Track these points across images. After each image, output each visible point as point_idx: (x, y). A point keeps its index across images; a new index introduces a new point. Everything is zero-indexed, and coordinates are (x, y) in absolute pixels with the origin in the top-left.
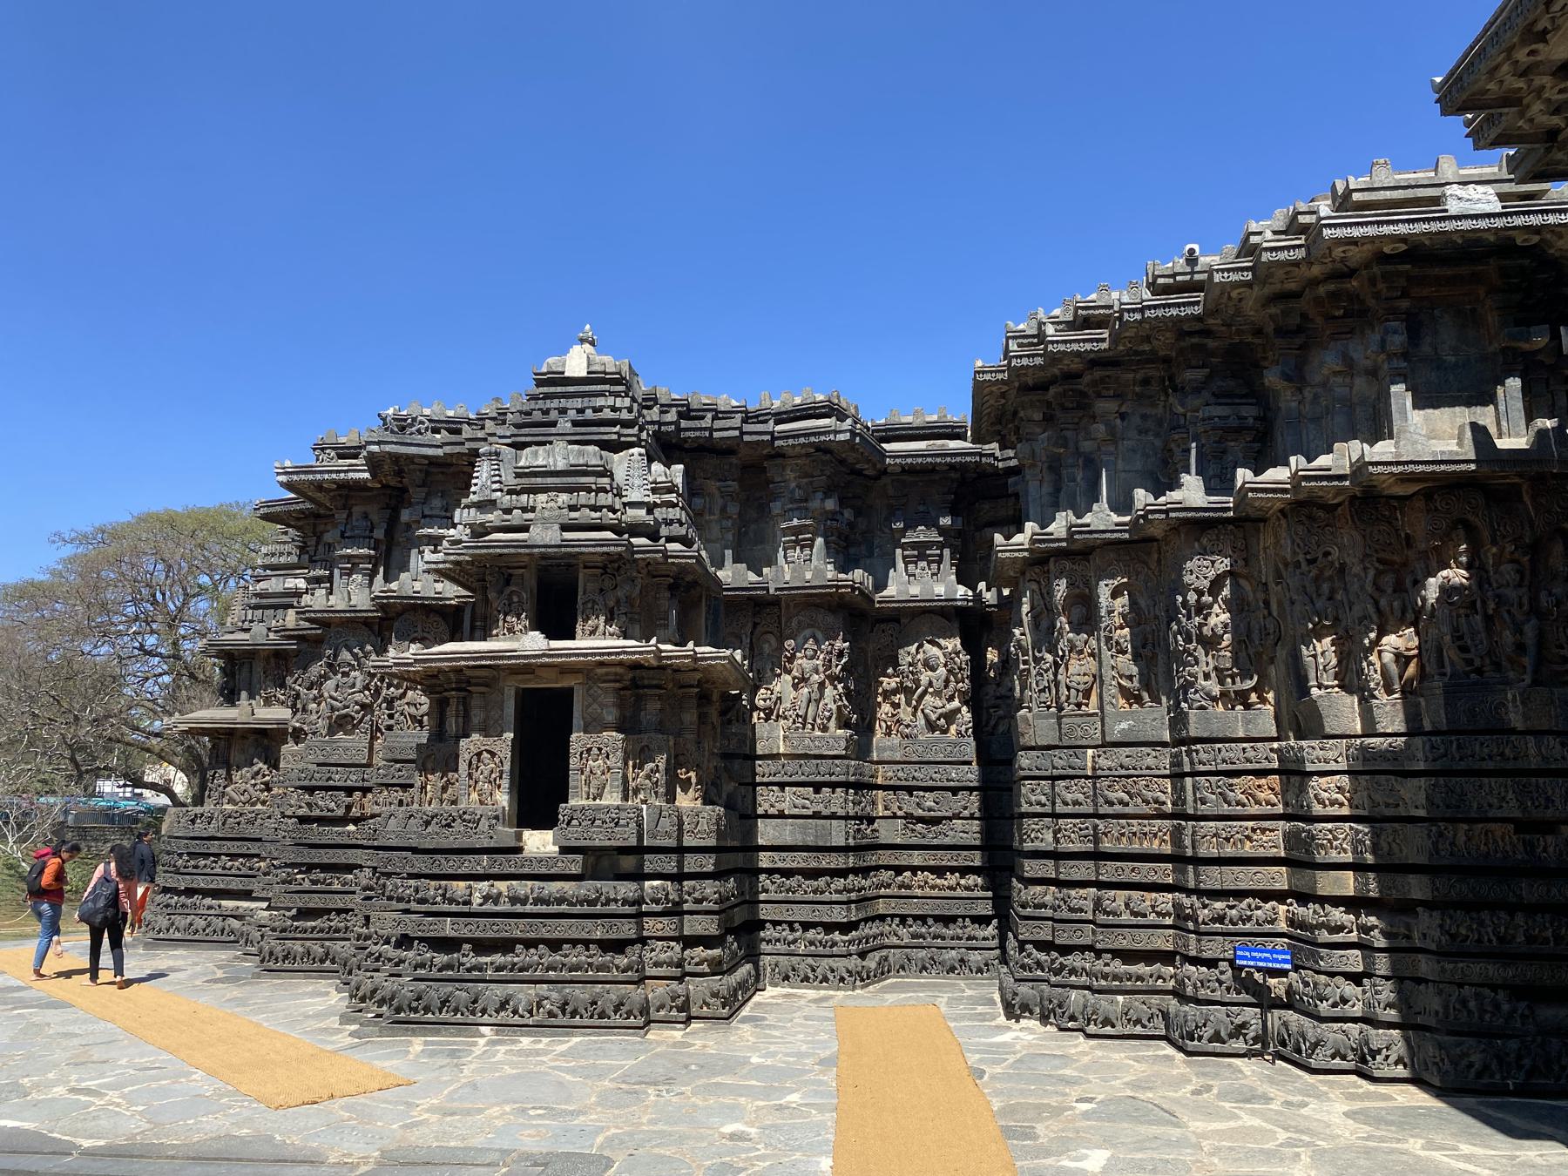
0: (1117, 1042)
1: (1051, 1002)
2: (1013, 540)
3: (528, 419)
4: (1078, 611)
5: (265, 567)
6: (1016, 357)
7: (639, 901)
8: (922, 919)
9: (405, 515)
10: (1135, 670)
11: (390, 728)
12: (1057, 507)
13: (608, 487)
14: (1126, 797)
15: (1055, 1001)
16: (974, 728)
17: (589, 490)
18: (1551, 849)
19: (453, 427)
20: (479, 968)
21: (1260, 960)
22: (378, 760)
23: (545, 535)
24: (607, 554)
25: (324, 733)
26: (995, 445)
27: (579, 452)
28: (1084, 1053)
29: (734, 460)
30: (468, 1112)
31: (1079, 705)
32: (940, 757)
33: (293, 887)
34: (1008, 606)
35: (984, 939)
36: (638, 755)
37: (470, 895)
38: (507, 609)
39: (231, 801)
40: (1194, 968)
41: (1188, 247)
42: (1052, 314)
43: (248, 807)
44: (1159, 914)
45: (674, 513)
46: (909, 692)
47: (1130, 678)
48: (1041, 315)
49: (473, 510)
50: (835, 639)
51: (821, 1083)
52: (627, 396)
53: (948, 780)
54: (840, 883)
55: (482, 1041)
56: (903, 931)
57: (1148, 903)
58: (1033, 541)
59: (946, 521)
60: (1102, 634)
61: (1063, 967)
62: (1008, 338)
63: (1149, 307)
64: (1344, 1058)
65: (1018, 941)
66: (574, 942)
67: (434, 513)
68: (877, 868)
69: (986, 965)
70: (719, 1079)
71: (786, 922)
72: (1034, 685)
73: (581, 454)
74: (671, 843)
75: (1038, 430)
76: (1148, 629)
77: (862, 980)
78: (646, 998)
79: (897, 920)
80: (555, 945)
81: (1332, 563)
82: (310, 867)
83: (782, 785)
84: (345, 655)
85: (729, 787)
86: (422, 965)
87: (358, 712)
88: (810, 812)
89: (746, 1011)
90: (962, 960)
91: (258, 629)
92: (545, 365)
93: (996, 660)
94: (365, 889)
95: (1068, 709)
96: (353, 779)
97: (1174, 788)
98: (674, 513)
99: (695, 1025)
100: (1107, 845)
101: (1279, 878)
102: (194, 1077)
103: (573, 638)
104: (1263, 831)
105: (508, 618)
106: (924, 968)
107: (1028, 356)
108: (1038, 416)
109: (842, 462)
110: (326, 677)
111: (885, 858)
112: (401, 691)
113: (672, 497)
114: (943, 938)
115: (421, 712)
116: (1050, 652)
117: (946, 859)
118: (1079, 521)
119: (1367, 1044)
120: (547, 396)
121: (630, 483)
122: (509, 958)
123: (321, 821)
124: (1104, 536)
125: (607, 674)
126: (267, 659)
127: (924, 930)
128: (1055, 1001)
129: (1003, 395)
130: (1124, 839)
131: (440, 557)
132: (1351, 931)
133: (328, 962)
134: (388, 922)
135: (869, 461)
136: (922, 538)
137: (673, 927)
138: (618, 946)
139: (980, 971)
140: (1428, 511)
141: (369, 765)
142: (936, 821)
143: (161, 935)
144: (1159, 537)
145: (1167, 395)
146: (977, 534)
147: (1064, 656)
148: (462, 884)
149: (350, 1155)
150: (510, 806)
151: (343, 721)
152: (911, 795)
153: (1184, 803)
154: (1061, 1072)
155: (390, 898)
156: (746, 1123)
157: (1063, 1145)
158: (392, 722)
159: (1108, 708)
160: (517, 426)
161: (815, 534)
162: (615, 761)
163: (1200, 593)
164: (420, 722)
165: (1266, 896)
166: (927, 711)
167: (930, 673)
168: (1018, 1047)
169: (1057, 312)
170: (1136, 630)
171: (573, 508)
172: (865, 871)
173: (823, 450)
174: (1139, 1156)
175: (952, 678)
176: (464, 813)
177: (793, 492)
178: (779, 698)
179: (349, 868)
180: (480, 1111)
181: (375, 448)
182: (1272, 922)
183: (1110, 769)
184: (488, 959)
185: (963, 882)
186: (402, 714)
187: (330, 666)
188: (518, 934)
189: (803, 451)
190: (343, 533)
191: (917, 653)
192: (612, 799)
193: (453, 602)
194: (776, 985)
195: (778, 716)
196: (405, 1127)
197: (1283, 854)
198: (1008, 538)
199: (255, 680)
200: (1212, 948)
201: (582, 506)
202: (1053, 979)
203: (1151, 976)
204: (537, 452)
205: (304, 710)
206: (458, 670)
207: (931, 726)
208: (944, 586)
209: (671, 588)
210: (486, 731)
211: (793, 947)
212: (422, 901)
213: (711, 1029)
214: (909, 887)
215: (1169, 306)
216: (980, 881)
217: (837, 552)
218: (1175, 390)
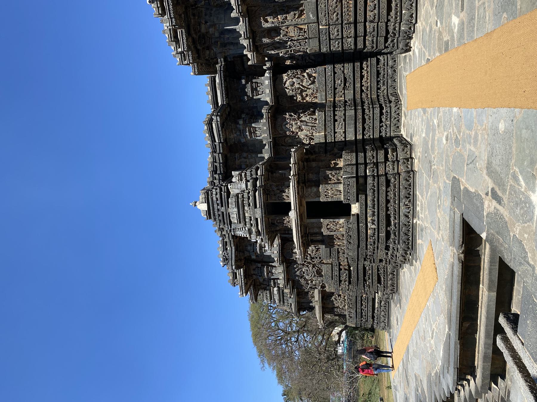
0: (418, 12)
1: (405, 36)
2: (250, 58)
4: (273, 34)
5: (271, 299)
6: (189, 61)
7: (374, 176)
8: (378, 82)
9: (254, 257)
10: (292, 13)
11: (320, 258)
12: (238, 43)
13: (242, 195)
14: (335, 14)
15: (405, 35)
16: (313, 68)
17: (243, 200)
19: (225, 244)
20: (395, 225)
22: (330, 261)
23: (259, 213)
24: (263, 193)
25: (322, 278)
26: (217, 66)
27: (231, 204)
28: (422, 24)
29: (229, 155)
30: (439, 223)
32: (324, 79)
33: (371, 285)
34: (271, 58)
35: (384, 60)
36: (326, 180)
37: (372, 228)
38: (282, 223)
39: (344, 306)
41: (148, 3)
42: (174, 49)
43: (346, 301)
45: (248, 173)
46: (302, 91)
47: (295, 14)
48: (174, 53)
49: (252, 236)
50: (285, 118)
51: (431, 113)
52: (212, 190)
53: (331, 76)
54: (367, 111)
55: (418, 222)
56: (382, 88)
57: (371, 4)
59: (243, 82)
60: (280, 25)
62: (183, 64)
63: (170, 16)
65: (384, 49)
67: (252, 248)
68: (361, 98)
69: (393, 59)
70: (430, 146)
71: (380, 129)
72: (299, 48)
73: (232, 204)
74: (355, 167)
75: (212, 52)
76: (278, 9)
77: (399, 101)
78: (404, 172)
79: (379, 91)
80: (388, 201)
82: (365, 280)
83: (335, 133)
84: (298, 273)
85: (336, 150)
86: (394, 242)
87: (315, 268)
88: (344, 123)
89: (409, 140)
90: (392, 68)
91: (290, 301)
92: (204, 216)
93: (290, 61)
94: (371, 263)
95: (306, 36)
96: (336, 268)
98: (248, 173)
99: (413, 156)
100: (352, 20)
102: (428, 305)
103: (290, 203)
105: (285, 223)
106: (394, 81)
107: (189, 57)
108: (208, 52)
109: (226, 119)
110: (305, 279)
111: (358, 96)
112: (308, 255)
113: (243, 174)
114: (384, 74)
115: (315, 249)
116: (287, 43)
117: (358, 75)
118: (243, 36)
121: (240, 188)
123: (350, 277)
124: (247, 27)
125: (301, 191)
126: (300, 298)
127: (382, 81)
128: (405, 35)
129: (201, 64)
131: (266, 245)
133: (394, 273)
134: (381, 254)
135: (225, 110)
136: (250, 90)
137: (382, 165)
138: (388, 182)
139: (395, 61)
141: (332, 264)
142: (345, 79)
144: (246, 7)
145: (198, 7)
146: (247, 70)
147: (288, 38)
148: (369, 231)
149: (451, 255)
150: (344, 219)
151: (319, 273)
152: (337, 88)
154: (428, 32)
155: (374, 253)
156: (443, 136)
157: (451, 31)
158: (318, 257)
159: (306, 22)
160: (224, 224)
161: (251, 127)
162: (329, 186)
166: (308, 84)
167: (295, 84)
168: (420, 47)
169: (173, 48)
170: (279, 13)
171: (249, 205)
172: (363, 103)
173: (223, 125)
174: (454, 5)
175: (297, 76)
176: (346, 232)
177: (237, 135)
178: (306, 135)
179: (364, 268)
180: (439, 219)
181: (234, 267)
183: (326, 20)
184: (392, 222)
185: (365, 69)
186: (316, 255)
187: (301, 278)
188: (384, 213)
189: (224, 132)
190: (260, 276)
191: (288, 89)
192: (341, 187)
193: (280, 241)
194: (400, 130)
195: (312, 136)
196: (443, 241)
198: (250, 60)
199: (307, 301)
201: (248, 202)
202: (397, 36)
204: (232, 217)
205: (315, 285)
207: (313, 82)
208: (266, 81)
209: (272, 173)
210: (321, 227)
211: (388, 126)
212: (374, 243)
213: (414, 150)
214: (368, 87)
215: (169, 9)
216: (365, 63)
217: (257, 119)
218: (196, 4)
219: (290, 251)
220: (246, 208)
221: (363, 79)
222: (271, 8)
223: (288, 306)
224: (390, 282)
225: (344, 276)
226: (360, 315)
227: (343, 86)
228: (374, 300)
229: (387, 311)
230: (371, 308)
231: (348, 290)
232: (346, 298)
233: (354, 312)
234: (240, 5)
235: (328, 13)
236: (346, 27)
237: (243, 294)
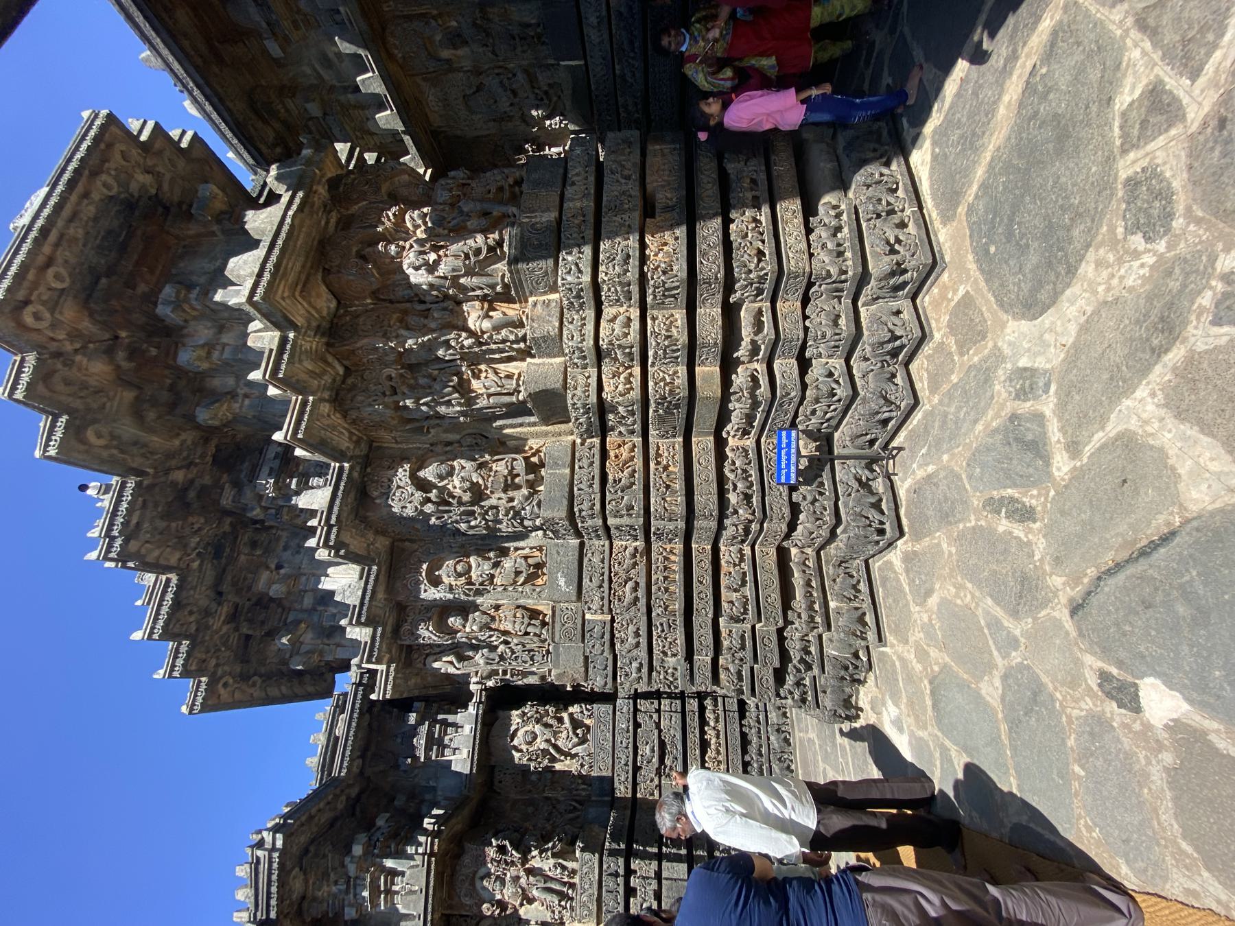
0: (883, 612)
14: (630, 584)
18: (669, 195)
21: (789, 460)
31: (544, 624)
32: (609, 736)
40: (800, 528)
44: (742, 560)
57: (731, 569)
58: (378, 662)
59: (412, 718)
61: (802, 661)
64: (894, 376)
81: (402, 376)
90: (778, 731)
97: (620, 538)
100: (678, 606)
101: (703, 444)
104: (658, 455)
114: (761, 746)
119: (882, 344)
127: (755, 765)
128: (843, 673)
130: (672, 588)
132: (756, 370)
136: (423, 742)
140: (339, 272)
142: (662, 744)
163: (428, 500)
165: (721, 457)
167: (538, 740)
182: (746, 451)
183: (602, 599)
185: (712, 724)
191: (521, 751)
197: (681, 439)
203: (804, 572)
207: (583, 741)
221: (707, 752)
222: (454, 550)
227: (657, 765)
234: (333, 526)
235: (611, 581)
236: (662, 624)
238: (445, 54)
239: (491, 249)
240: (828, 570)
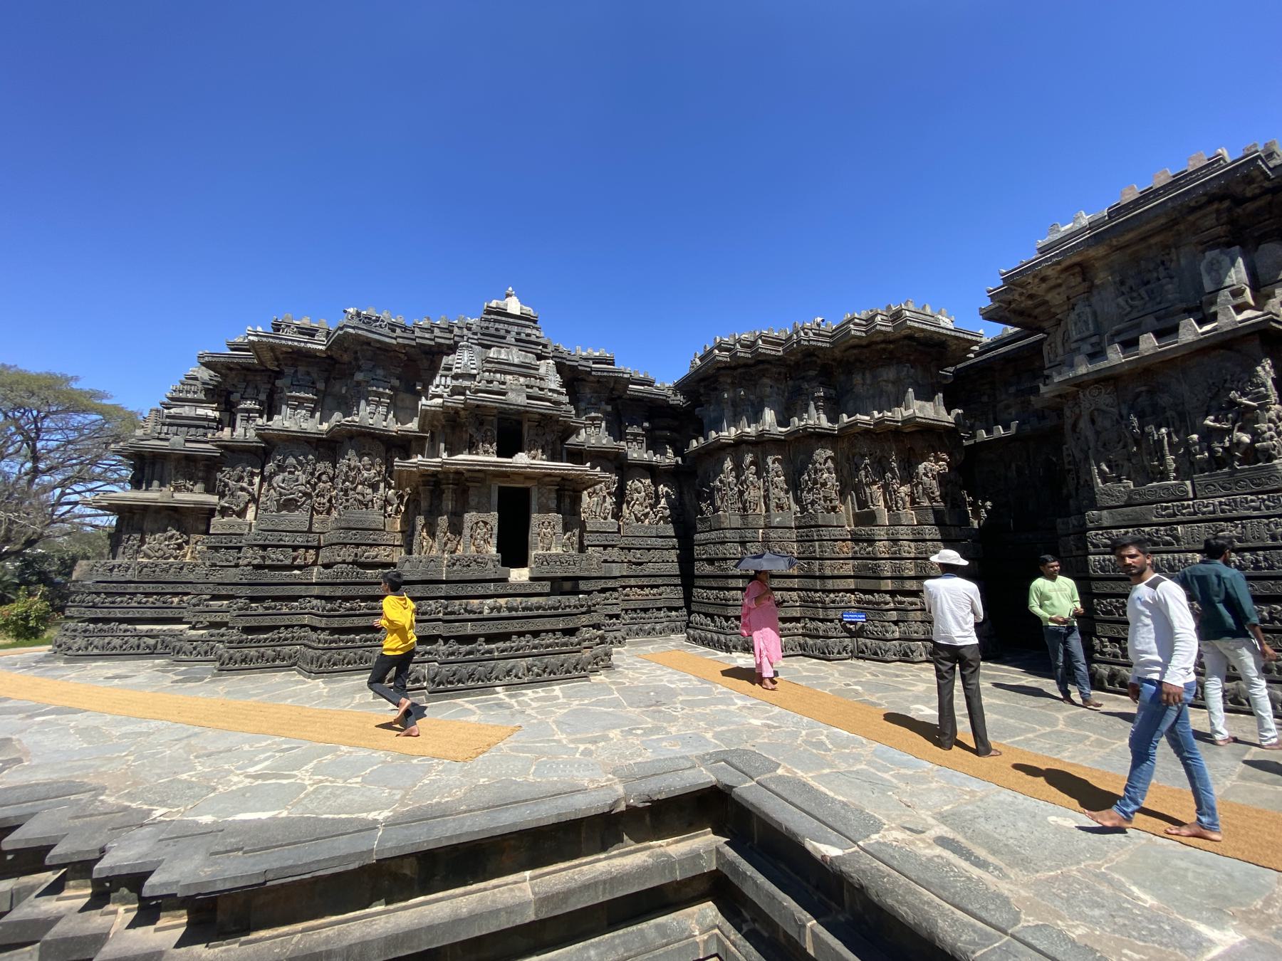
3: (486, 331)
8: (635, 610)
20: (490, 652)
32: (642, 534)
59: (646, 424)
66: (547, 631)
73: (526, 357)
80: (536, 634)
84: (291, 460)
86: (452, 654)
87: (301, 497)
96: (300, 540)
101: (851, 584)
108: (729, 381)
110: (275, 474)
117: (645, 581)
120: (495, 321)
122: (508, 644)
138: (570, 632)
141: (310, 531)
142: (640, 564)
143: (80, 652)
153: (814, 552)
162: (559, 529)
164: (366, 506)
165: (847, 591)
179: (295, 598)
181: (351, 330)
184: (493, 646)
187: (278, 466)
188: (511, 629)
200: (832, 614)
206: (458, 473)
207: (638, 519)
219: (366, 451)
220: (522, 380)
223: (160, 433)
224: (253, 652)
225: (275, 556)
226: (115, 590)
228: (179, 621)
229: (126, 652)
230: (137, 615)
231: (214, 565)
232: (172, 560)
233: (128, 577)
237: (257, 335)
238: (1013, 466)
239: (934, 498)
240: (796, 638)
